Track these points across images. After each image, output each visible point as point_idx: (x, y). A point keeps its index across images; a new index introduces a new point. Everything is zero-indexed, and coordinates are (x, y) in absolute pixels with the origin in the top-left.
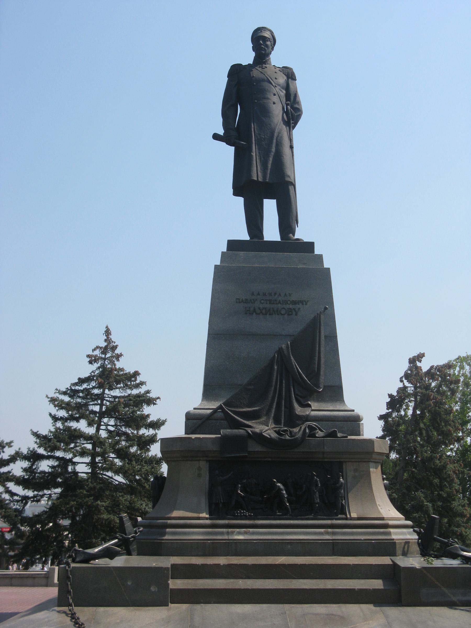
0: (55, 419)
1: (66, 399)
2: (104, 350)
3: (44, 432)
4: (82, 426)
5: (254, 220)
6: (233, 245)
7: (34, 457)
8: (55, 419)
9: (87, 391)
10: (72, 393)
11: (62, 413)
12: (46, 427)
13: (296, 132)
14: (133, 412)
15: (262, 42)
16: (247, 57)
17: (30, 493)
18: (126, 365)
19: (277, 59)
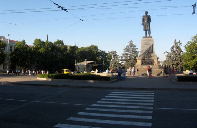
0: (124, 52)
1: (125, 49)
2: (130, 42)
3: (123, 53)
4: (128, 53)
5: (146, 33)
6: (143, 37)
7: (122, 57)
8: (124, 52)
9: (129, 48)
10: (126, 48)
11: (125, 51)
12: (123, 53)
13: (151, 23)
14: (135, 52)
15: (147, 13)
16: (145, 14)
17: (122, 62)
18: (134, 43)
19: (148, 14)
